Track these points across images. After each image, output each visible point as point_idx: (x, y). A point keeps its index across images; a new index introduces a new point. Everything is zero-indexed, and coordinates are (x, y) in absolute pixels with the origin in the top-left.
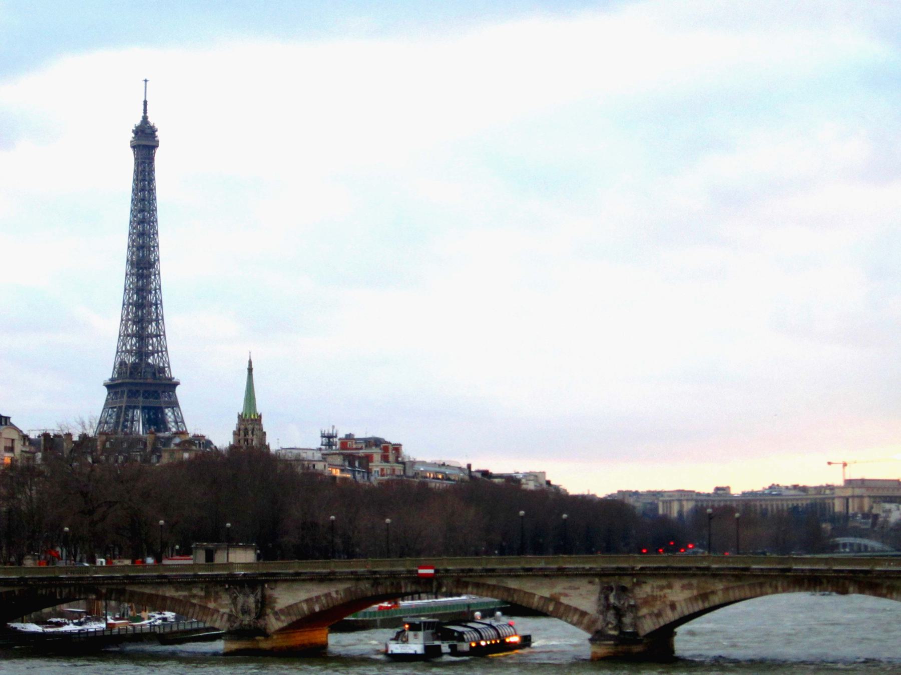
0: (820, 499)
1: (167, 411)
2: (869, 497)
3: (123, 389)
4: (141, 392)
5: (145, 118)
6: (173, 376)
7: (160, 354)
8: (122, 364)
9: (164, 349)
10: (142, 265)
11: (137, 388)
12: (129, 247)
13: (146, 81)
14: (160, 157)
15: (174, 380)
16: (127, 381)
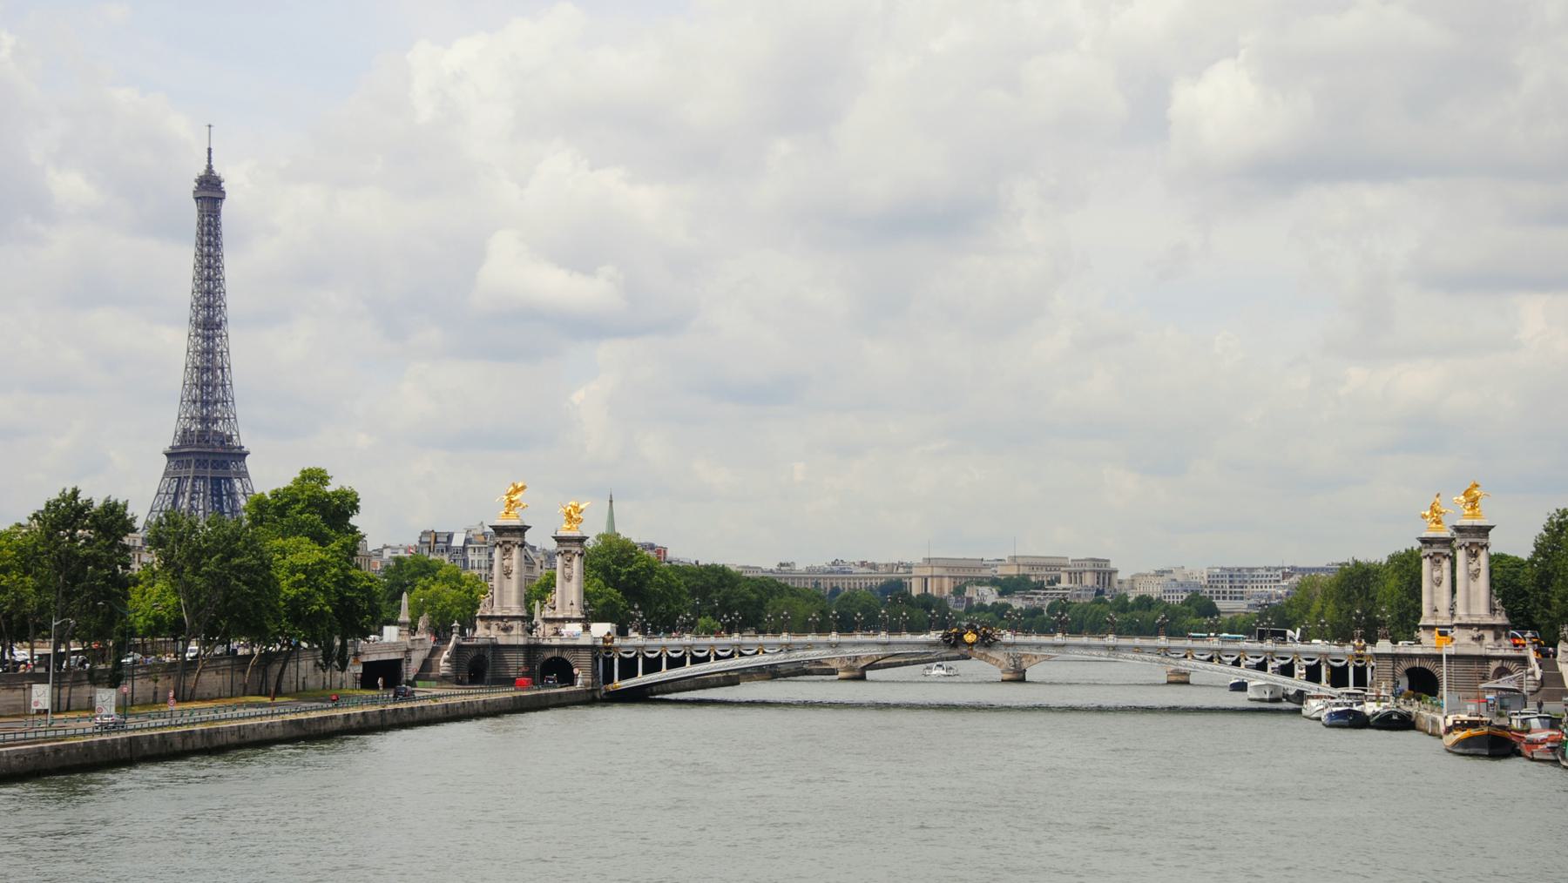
0: (896, 578)
1: (235, 480)
2: (950, 577)
3: (189, 458)
4: (210, 461)
5: (210, 167)
6: (242, 445)
7: (227, 420)
8: (184, 431)
9: (232, 416)
10: (209, 327)
11: (206, 457)
12: (192, 306)
13: (210, 126)
14: (227, 209)
15: (245, 450)
16: (194, 450)
